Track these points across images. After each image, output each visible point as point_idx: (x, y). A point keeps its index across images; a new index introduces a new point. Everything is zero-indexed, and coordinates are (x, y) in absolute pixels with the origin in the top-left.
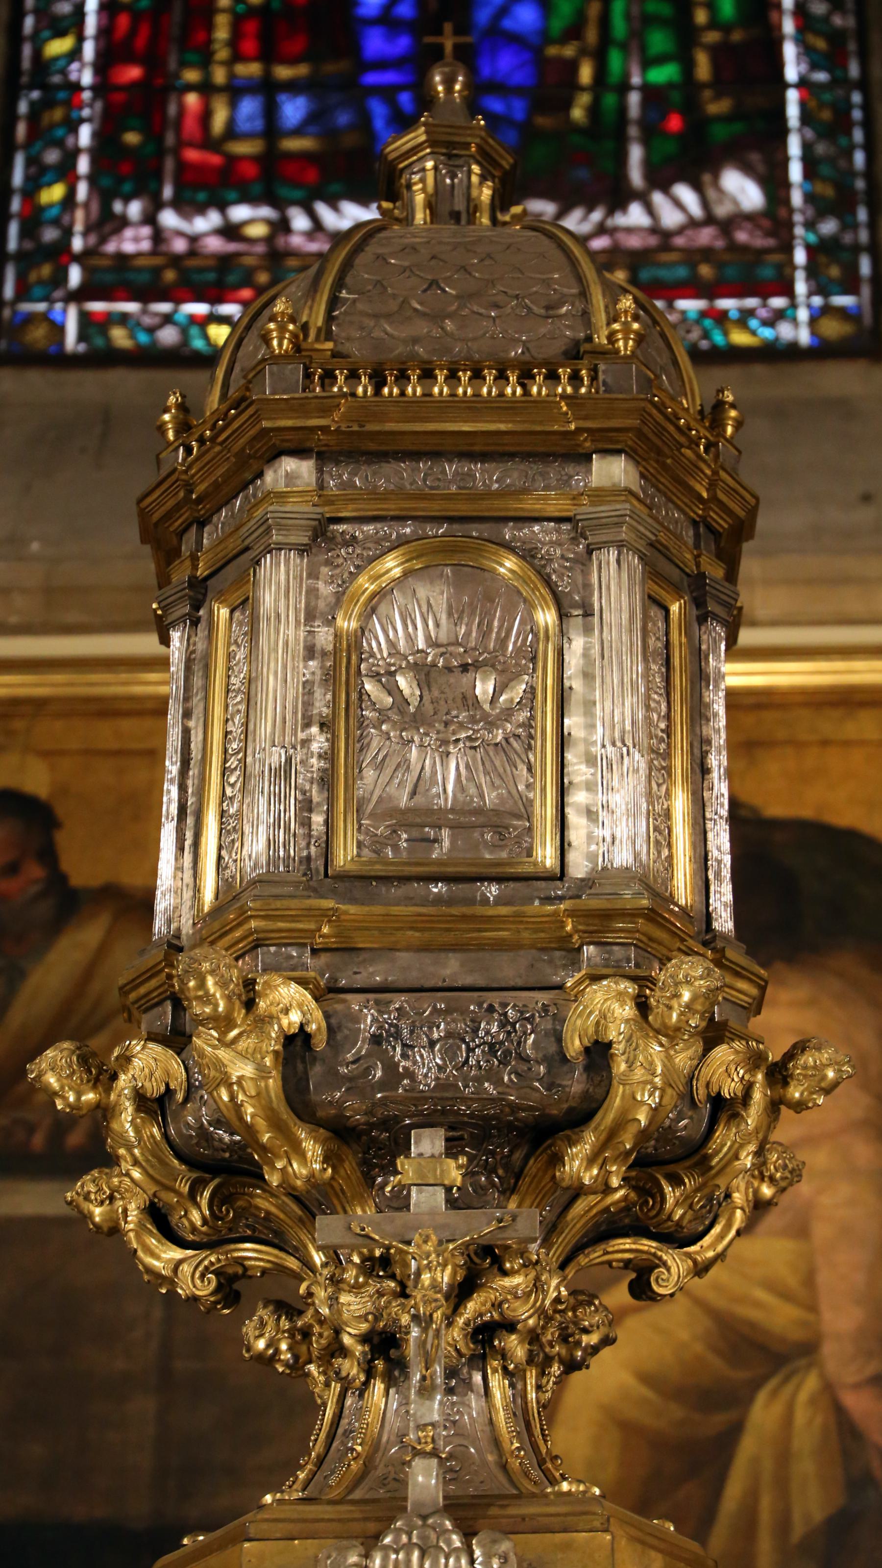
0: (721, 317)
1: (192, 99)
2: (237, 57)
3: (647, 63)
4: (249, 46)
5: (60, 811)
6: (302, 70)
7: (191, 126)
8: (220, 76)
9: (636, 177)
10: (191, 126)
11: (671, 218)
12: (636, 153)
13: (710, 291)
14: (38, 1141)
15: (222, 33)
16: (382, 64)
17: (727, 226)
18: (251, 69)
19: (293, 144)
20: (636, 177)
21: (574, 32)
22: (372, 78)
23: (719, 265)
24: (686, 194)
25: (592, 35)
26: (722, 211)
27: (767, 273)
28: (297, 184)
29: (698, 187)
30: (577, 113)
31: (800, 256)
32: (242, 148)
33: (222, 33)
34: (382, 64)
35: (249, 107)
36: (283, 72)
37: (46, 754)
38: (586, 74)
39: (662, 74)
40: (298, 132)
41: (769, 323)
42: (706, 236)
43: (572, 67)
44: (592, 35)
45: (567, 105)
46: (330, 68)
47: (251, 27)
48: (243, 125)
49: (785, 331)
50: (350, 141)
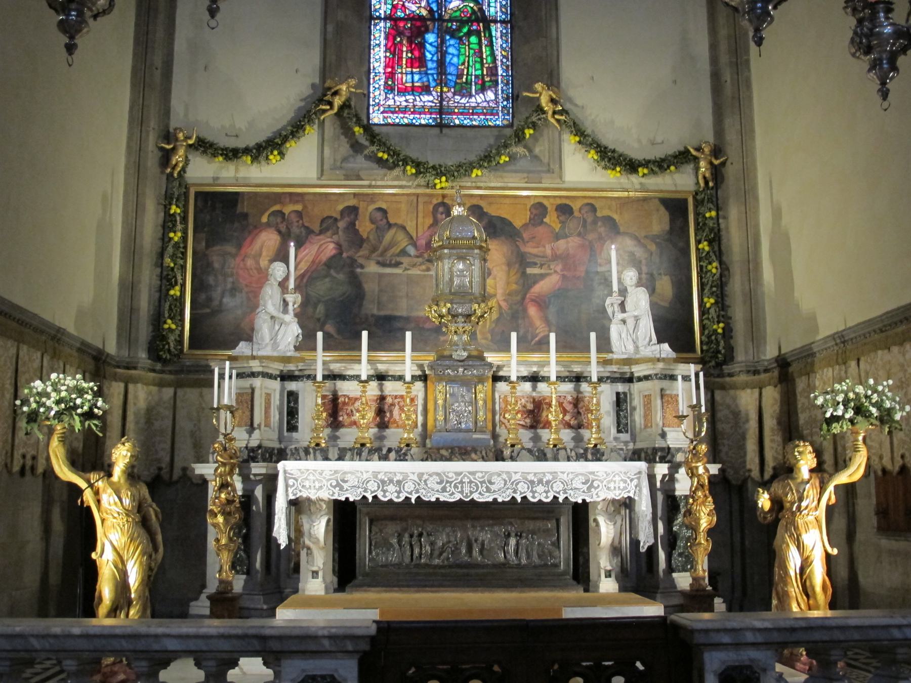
0: (487, 120)
1: (400, 75)
2: (407, 67)
3: (475, 70)
4: (409, 65)
5: (388, 211)
6: (418, 70)
7: (400, 81)
8: (404, 72)
9: (474, 93)
10: (400, 81)
11: (479, 100)
12: (473, 87)
13: (485, 114)
14: (388, 262)
15: (404, 62)
16: (431, 69)
17: (488, 102)
18: (409, 70)
19: (416, 84)
20: (474, 93)
21: (463, 64)
22: (429, 72)
23: (487, 110)
24: (481, 95)
25: (466, 64)
26: (487, 99)
27: (495, 111)
28: (417, 92)
29: (484, 95)
30: (464, 80)
31: (500, 109)
32: (408, 85)
33: (404, 62)
34: (431, 69)
35: (409, 77)
36: (414, 70)
37: (386, 202)
38: (465, 73)
39: (479, 73)
40: (417, 82)
41: (495, 121)
42: (485, 104)
43: (463, 70)
44: (466, 64)
45: (462, 78)
46: (422, 69)
47: (409, 61)
48: (408, 81)
49: (498, 123)
50: (426, 84)
